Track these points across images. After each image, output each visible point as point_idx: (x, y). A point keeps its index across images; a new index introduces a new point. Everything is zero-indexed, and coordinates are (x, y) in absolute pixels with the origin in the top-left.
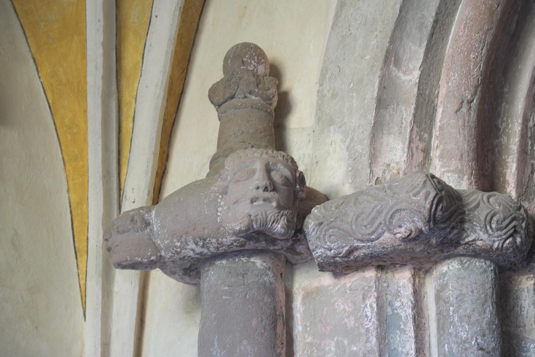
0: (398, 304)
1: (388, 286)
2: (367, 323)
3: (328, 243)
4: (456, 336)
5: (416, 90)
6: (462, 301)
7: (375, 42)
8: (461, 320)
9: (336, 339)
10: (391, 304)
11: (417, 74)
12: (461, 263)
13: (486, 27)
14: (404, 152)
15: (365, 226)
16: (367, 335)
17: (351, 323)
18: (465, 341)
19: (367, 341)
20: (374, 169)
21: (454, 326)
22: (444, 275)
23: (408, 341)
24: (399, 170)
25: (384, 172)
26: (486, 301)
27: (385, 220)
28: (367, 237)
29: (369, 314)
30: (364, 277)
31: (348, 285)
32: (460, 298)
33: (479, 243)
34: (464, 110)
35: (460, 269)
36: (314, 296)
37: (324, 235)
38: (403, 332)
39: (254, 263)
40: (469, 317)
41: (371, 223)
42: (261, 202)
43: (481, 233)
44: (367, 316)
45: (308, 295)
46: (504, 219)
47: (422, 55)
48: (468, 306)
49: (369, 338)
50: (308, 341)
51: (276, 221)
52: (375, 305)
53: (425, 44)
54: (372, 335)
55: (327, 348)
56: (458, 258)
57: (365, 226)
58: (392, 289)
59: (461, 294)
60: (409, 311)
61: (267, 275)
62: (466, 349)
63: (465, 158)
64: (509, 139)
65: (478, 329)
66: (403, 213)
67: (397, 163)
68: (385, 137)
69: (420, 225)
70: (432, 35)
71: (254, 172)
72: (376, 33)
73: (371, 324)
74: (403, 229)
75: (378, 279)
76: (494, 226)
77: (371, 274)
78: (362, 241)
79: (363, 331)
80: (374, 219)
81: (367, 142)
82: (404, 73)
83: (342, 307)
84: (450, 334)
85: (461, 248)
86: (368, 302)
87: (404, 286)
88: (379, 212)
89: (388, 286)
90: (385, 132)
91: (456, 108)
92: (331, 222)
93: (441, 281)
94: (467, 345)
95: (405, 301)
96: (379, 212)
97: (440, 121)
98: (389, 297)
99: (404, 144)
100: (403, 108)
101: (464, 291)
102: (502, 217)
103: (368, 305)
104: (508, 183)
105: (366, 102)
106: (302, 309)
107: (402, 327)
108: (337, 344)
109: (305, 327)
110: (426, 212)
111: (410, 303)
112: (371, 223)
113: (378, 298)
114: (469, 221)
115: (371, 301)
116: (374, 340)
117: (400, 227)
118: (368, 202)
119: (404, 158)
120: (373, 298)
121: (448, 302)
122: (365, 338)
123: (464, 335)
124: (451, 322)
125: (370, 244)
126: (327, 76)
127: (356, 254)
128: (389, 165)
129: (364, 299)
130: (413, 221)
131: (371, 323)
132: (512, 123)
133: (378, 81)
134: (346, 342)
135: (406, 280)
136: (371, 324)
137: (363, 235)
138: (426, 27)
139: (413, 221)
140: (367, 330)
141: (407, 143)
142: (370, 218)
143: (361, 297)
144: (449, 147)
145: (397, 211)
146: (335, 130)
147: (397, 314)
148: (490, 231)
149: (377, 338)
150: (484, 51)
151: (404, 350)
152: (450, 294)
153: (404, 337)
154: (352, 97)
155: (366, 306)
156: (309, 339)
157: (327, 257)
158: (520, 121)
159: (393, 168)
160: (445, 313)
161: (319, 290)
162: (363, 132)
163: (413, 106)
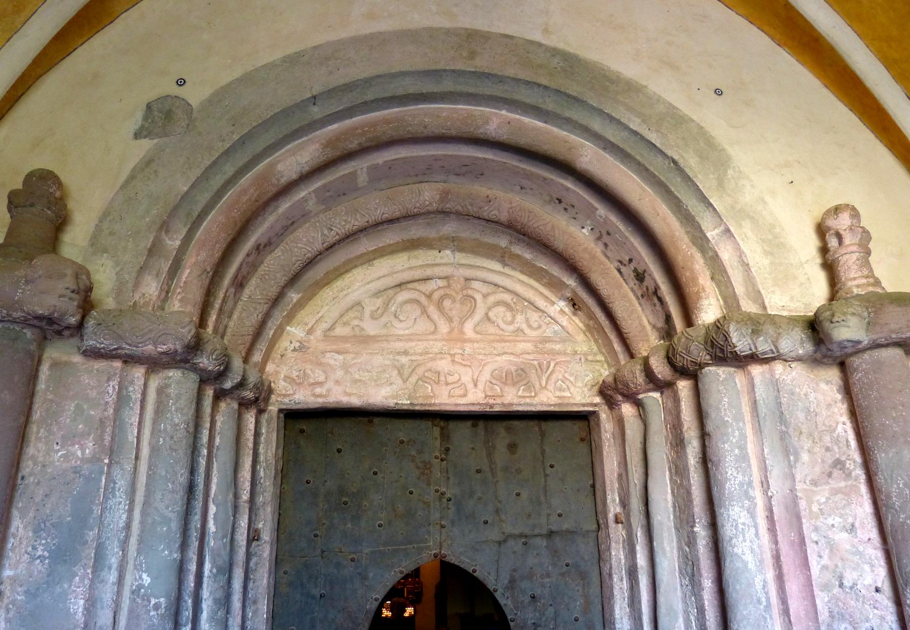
0: (131, 389)
1: (127, 375)
2: (107, 397)
3: (102, 339)
4: (171, 420)
5: (175, 252)
6: (180, 398)
7: (155, 212)
8: (176, 410)
9: (76, 402)
10: (127, 389)
11: (178, 243)
12: (183, 373)
13: (230, 232)
14: (157, 290)
15: (137, 337)
16: (105, 406)
17: (93, 394)
18: (177, 425)
19: (105, 410)
20: (135, 294)
21: (171, 413)
22: (170, 378)
23: (134, 416)
24: (150, 300)
25: (140, 298)
26: (193, 401)
27: (154, 337)
28: (136, 344)
29: (110, 392)
30: (111, 366)
31: (96, 367)
32: (178, 397)
33: (201, 365)
34: (204, 276)
35: (181, 377)
36: (62, 366)
37: (101, 333)
38: (131, 408)
39: (25, 333)
40: (182, 409)
41: (143, 336)
42: (66, 299)
43: (205, 359)
44: (108, 392)
45: (55, 365)
46: (220, 354)
47: (185, 233)
48: (183, 402)
49: (107, 408)
50: (49, 397)
51: (73, 316)
52: (117, 387)
53: (189, 226)
54: (110, 407)
55: (66, 407)
56: (182, 370)
57: (137, 337)
58: (129, 378)
59: (180, 394)
60: (139, 396)
61: (33, 344)
62: (177, 430)
63: (197, 306)
64: (215, 300)
65: (185, 418)
66: (169, 337)
67: (150, 295)
68: (146, 275)
69: (179, 348)
70: (194, 222)
71: (65, 275)
72: (158, 207)
73: (111, 399)
74: (165, 347)
75: (122, 369)
76: (214, 357)
77: (118, 364)
78: (130, 345)
79: (102, 402)
80: (147, 333)
81: (134, 275)
82: (169, 239)
83: (87, 381)
84: (167, 418)
85: (188, 365)
86: (111, 384)
87: (138, 377)
88: (151, 331)
89: (127, 375)
90: (147, 272)
91: (199, 273)
92: (109, 326)
93: (167, 381)
94: (178, 428)
95: (136, 388)
96: (151, 331)
97: (186, 278)
98: (126, 383)
99: (158, 284)
100: (163, 261)
101: (182, 392)
102: (220, 352)
103: (111, 386)
104: (208, 327)
105: (140, 248)
106: (47, 373)
107: (131, 405)
108: (77, 406)
109: (48, 387)
110: (186, 341)
111: (140, 390)
112: (143, 336)
113: (119, 382)
114: (201, 350)
115: (114, 383)
116: (111, 411)
117: (164, 345)
118: (143, 321)
119: (156, 293)
120: (116, 381)
121: (169, 397)
122: (103, 407)
123: (177, 421)
124: (169, 410)
125: (134, 348)
126: (108, 218)
127: (119, 351)
128: (144, 295)
129: (108, 380)
130: (175, 344)
131: (111, 398)
132: (219, 290)
133: (152, 238)
134: (85, 407)
135: (140, 374)
136: (111, 399)
137: (132, 342)
138: (192, 216)
139: (175, 344)
140: (107, 403)
141: (160, 284)
142: (141, 333)
143: (106, 378)
144: (188, 296)
145: (165, 334)
146: (108, 257)
147: (129, 395)
148: (211, 360)
149: (114, 410)
150: (224, 245)
151: (129, 421)
152: (172, 391)
153: (131, 412)
154: (129, 241)
155: (109, 386)
156: (50, 397)
157: (96, 347)
158: (224, 291)
159: (147, 297)
160: (165, 403)
161: (67, 364)
162: (132, 267)
163: (170, 262)
